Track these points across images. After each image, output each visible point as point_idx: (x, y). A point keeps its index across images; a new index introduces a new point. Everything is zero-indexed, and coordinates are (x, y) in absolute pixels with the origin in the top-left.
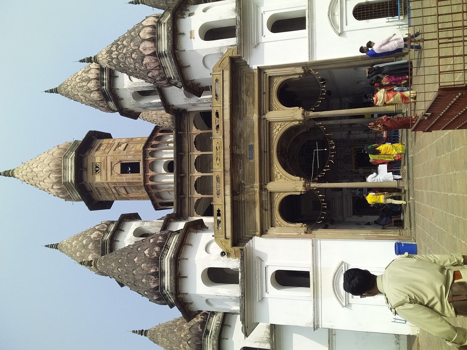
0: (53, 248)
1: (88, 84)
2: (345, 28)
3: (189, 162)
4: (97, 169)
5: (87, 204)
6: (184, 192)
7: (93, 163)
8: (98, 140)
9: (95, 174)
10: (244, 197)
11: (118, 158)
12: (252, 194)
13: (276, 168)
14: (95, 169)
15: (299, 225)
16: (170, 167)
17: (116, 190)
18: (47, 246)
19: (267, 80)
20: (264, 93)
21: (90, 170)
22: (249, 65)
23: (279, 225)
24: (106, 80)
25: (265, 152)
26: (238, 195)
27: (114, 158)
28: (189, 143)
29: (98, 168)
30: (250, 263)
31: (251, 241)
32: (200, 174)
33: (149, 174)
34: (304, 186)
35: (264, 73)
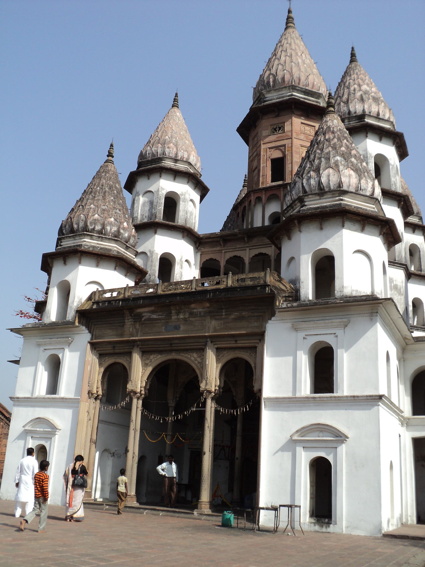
0: (174, 102)
1: (343, 102)
3: (259, 245)
9: (272, 128)
10: (129, 323)
11: (290, 153)
12: (130, 331)
13: (156, 359)
14: (278, 127)
18: (176, 95)
19: (252, 344)
20: (236, 341)
21: (276, 121)
22: (270, 319)
23: (101, 362)
24: (349, 124)
25: (171, 344)
26: (131, 316)
27: (290, 147)
29: (279, 131)
30: (69, 331)
31: (87, 331)
32: (247, 261)
33: (264, 195)
35: (260, 340)
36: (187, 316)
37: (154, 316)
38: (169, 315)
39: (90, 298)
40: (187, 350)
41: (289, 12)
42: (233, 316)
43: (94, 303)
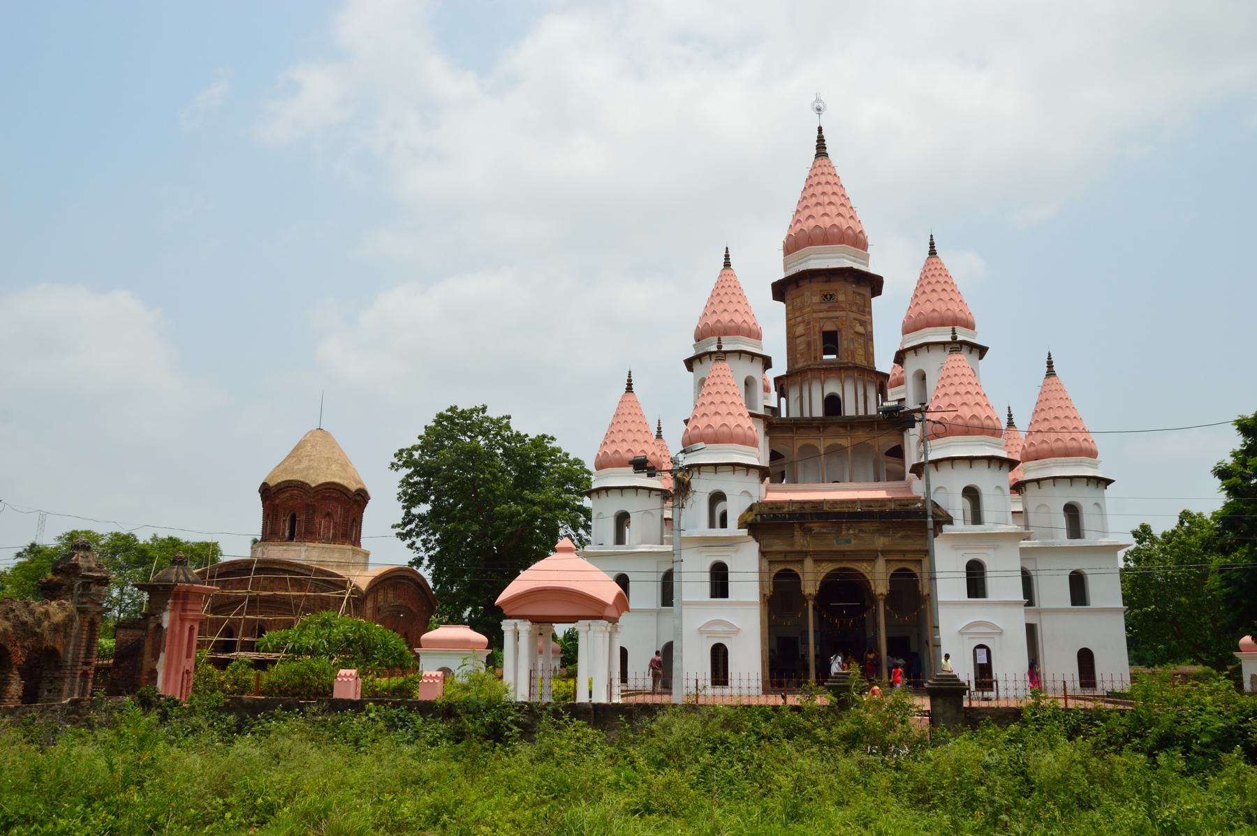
2: (966, 637)
4: (828, 297)
5: (780, 281)
6: (802, 430)
7: (836, 290)
8: (869, 289)
10: (798, 534)
15: (772, 589)
16: (833, 404)
17: (799, 323)
26: (800, 528)
28: (861, 435)
34: (810, 594)
36: (857, 532)
37: (825, 530)
38: (840, 532)
39: (751, 509)
40: (858, 561)
41: (820, 129)
42: (899, 535)
43: (756, 515)
